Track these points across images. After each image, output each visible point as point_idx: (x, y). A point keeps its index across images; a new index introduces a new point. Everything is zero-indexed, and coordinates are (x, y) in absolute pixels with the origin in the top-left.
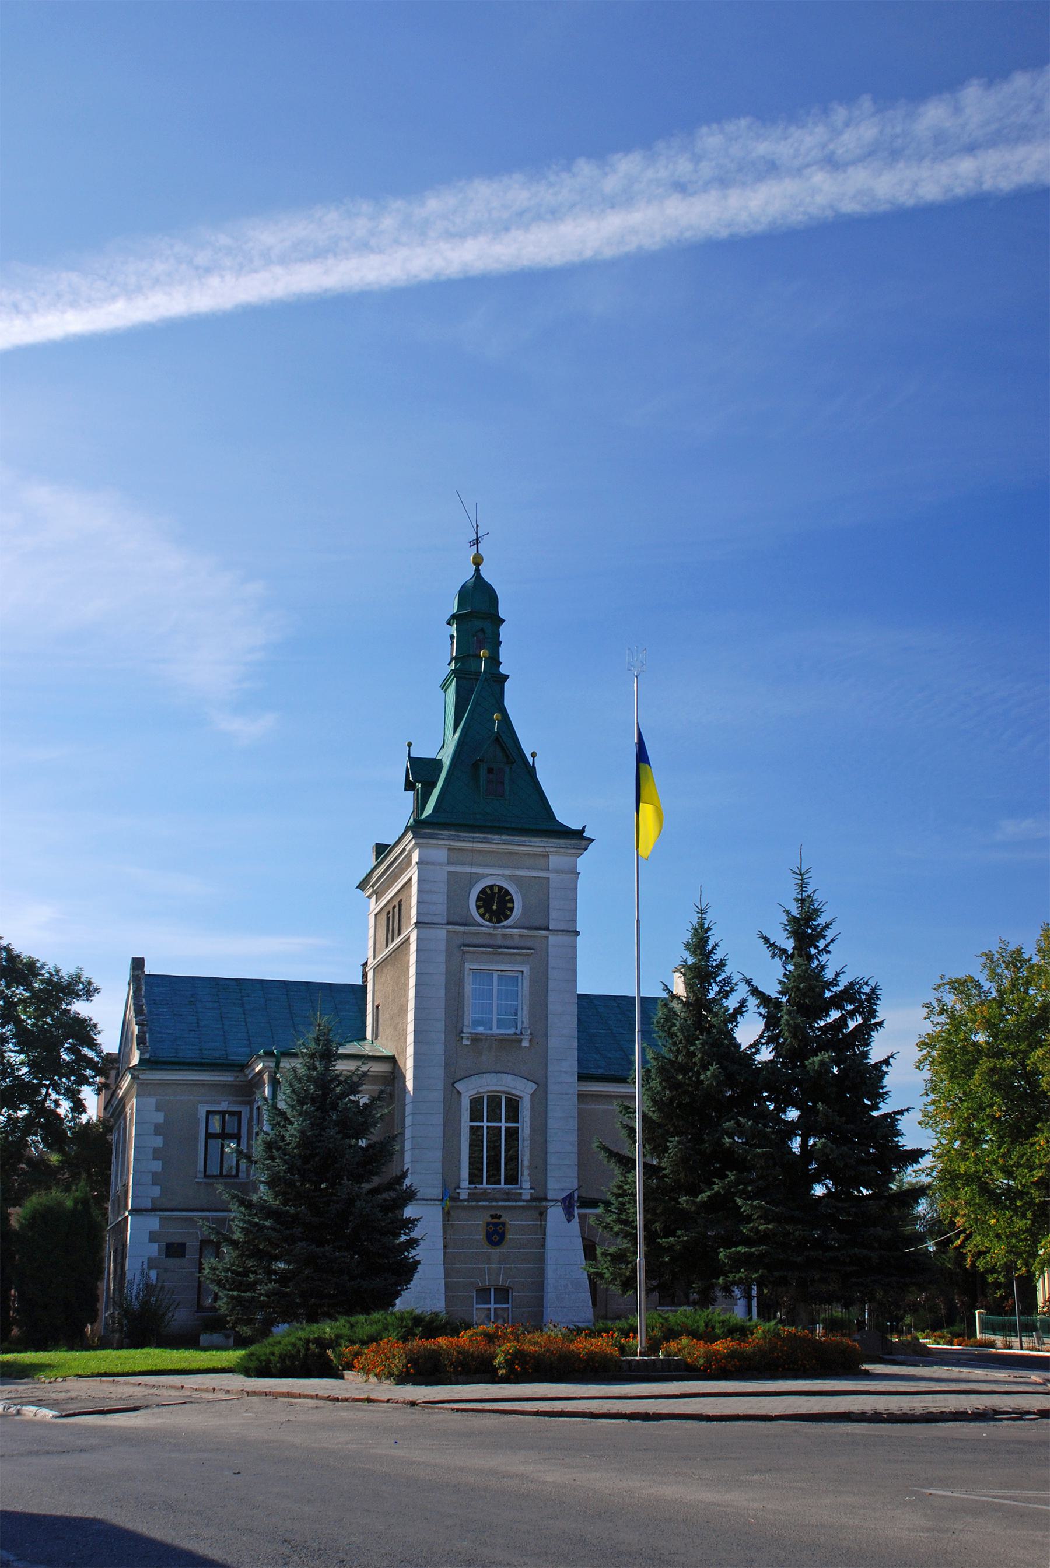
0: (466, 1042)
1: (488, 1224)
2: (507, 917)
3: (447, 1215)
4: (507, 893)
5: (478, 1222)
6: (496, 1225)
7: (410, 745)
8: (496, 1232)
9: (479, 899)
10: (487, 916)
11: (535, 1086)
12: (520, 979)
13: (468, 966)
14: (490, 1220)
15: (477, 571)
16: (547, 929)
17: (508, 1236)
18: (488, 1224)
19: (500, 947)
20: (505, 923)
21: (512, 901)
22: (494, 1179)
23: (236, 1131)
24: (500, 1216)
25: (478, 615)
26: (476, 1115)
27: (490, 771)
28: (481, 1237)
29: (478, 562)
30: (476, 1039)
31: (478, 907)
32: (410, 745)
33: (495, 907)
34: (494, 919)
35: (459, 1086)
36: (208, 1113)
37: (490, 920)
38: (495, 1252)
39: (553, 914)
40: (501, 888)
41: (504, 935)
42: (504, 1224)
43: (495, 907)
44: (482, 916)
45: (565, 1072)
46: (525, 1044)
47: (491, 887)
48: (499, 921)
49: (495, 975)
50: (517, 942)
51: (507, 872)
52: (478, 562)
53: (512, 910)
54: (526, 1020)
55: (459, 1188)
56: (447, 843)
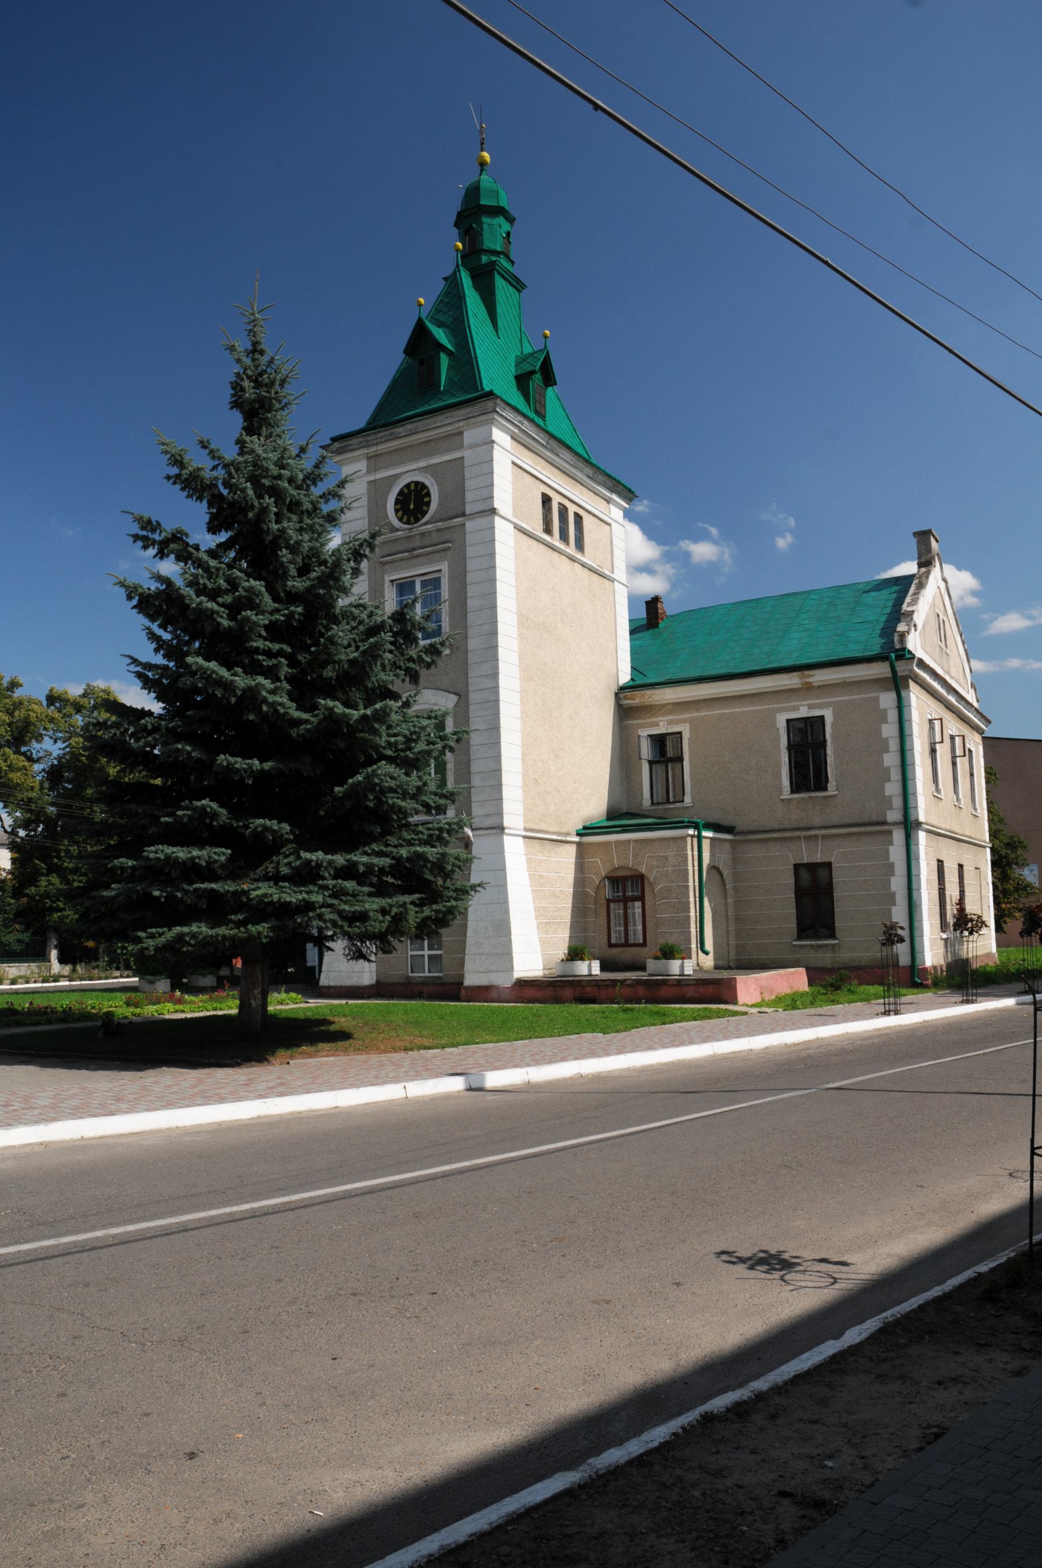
2: (424, 513)
9: (397, 502)
11: (455, 698)
13: (387, 578)
16: (463, 515)
19: (414, 549)
20: (424, 520)
21: (428, 494)
23: (654, 766)
31: (397, 511)
33: (412, 507)
37: (408, 523)
40: (417, 483)
41: (423, 534)
43: (412, 507)
44: (400, 520)
45: (487, 676)
47: (408, 486)
48: (417, 520)
50: (435, 537)
51: (422, 464)
53: (428, 504)
56: (360, 452)
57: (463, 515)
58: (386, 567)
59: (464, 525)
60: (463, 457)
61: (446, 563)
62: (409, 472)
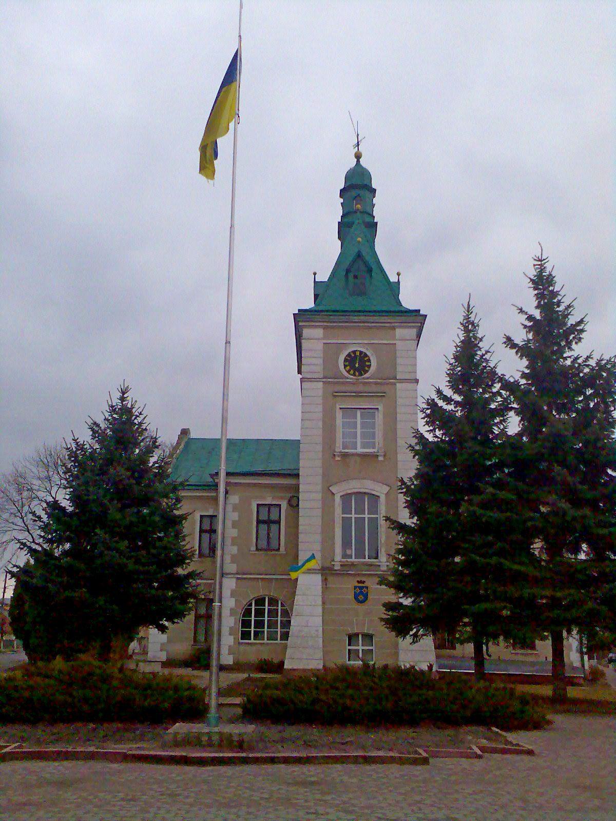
0: (337, 458)
1: (355, 587)
2: (366, 372)
3: (325, 581)
4: (366, 355)
5: (348, 585)
6: (361, 588)
7: (315, 274)
8: (361, 593)
9: (345, 360)
10: (352, 372)
11: (388, 488)
12: (376, 413)
13: (338, 407)
14: (357, 584)
15: (358, 161)
16: (395, 378)
17: (370, 597)
18: (355, 587)
21: (369, 361)
22: (360, 553)
24: (364, 582)
25: (358, 189)
26: (346, 509)
27: (356, 277)
28: (352, 597)
29: (358, 156)
30: (345, 456)
31: (345, 366)
32: (315, 274)
33: (357, 365)
34: (357, 373)
35: (333, 489)
36: (202, 517)
38: (362, 608)
39: (399, 369)
40: (361, 352)
42: (367, 587)
43: (357, 365)
44: (348, 372)
46: (381, 458)
47: (354, 352)
48: (361, 375)
49: (359, 413)
52: (358, 156)
53: (369, 366)
54: (381, 442)
55: (333, 560)
57: (395, 378)
58: (337, 398)
59: (395, 384)
60: (395, 344)
61: (382, 405)
62: (356, 343)
